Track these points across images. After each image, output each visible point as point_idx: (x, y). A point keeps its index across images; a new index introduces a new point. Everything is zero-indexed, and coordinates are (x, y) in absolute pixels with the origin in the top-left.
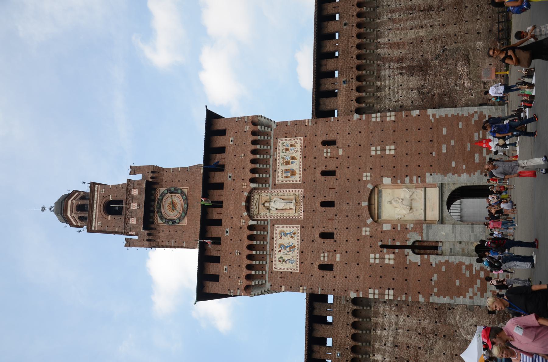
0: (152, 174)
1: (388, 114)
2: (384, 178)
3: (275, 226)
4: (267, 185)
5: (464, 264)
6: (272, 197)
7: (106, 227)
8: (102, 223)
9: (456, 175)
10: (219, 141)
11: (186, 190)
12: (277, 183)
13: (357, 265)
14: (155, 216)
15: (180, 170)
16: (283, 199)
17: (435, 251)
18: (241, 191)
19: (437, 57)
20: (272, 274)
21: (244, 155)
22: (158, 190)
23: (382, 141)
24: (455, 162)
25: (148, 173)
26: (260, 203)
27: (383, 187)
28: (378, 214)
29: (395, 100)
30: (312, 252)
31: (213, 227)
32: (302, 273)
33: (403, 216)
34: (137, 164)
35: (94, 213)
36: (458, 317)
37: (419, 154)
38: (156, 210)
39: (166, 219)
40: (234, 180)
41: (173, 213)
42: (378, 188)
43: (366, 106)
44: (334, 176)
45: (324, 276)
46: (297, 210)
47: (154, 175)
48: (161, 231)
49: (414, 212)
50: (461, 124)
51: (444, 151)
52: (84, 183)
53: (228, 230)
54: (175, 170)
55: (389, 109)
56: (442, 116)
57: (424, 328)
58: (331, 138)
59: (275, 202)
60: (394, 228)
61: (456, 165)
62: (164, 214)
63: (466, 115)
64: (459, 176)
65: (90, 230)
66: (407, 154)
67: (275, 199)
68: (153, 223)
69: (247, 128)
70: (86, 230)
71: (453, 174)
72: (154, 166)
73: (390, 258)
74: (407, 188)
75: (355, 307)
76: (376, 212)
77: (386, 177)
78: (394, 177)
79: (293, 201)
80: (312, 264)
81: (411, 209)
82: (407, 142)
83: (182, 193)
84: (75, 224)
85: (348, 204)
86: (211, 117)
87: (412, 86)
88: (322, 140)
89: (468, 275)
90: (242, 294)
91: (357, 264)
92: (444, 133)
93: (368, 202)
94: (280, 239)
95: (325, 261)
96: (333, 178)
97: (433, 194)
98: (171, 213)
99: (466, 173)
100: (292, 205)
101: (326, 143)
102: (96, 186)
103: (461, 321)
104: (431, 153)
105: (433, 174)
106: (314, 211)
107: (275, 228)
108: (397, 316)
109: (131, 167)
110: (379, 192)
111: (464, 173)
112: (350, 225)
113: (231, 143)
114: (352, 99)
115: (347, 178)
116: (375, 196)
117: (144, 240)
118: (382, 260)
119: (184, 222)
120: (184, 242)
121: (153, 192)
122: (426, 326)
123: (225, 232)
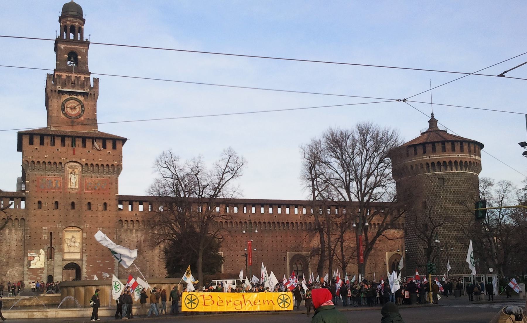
1: (118, 236)
5: (43, 271)
6: (77, 175)
7: (60, 53)
8: (62, 49)
9: (86, 267)
10: (109, 145)
11: (82, 118)
16: (76, 182)
19: (144, 258)
36: (17, 268)
38: (71, 97)
47: (92, 96)
48: (58, 100)
52: (90, 35)
53: (59, 150)
54: (95, 111)
57: (11, 253)
59: (75, 177)
62: (68, 102)
63: (115, 271)
64: (85, 268)
71: (86, 266)
79: (75, 187)
83: (80, 115)
86: (124, 141)
87: (131, 247)
89: (38, 272)
92: (106, 262)
97: (78, 256)
100: (73, 187)
101: (105, 204)
103: (16, 269)
104: (97, 256)
108: (16, 240)
110: (79, 231)
113: (108, 152)
119: (63, 116)
122: (12, 254)
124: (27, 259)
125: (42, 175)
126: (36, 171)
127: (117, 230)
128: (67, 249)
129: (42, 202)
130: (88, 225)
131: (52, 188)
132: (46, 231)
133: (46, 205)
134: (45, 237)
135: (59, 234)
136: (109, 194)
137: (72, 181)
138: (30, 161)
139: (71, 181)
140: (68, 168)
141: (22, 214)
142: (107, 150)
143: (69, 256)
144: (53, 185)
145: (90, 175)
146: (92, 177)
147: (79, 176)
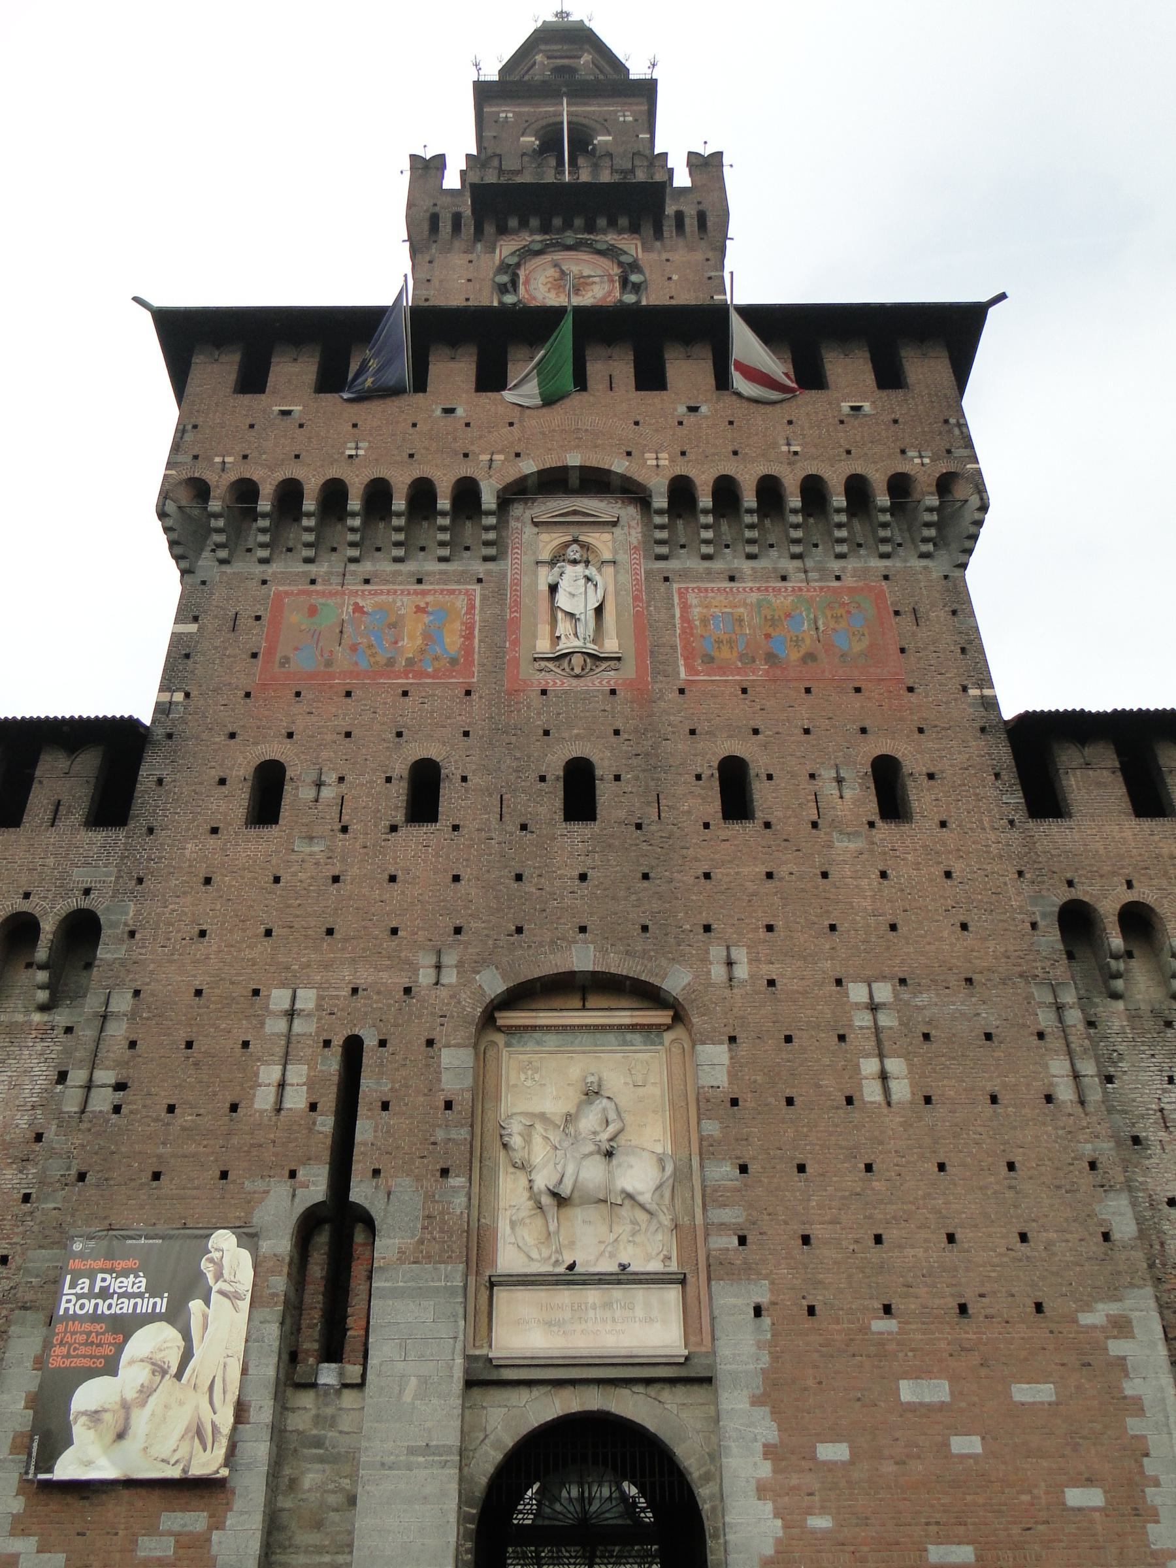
0: (694, 212)
2: (725, 1047)
3: (478, 587)
4: (664, 550)
5: (217, 1524)
6: (609, 570)
7: (495, 134)
12: (675, 586)
13: (262, 929)
14: (532, 234)
15: (715, 297)
16: (599, 611)
17: (316, 1346)
18: (629, 450)
20: (253, 584)
21: (796, 453)
22: (633, 239)
23: (926, 1037)
24: (843, 1463)
26: (584, 529)
27: (676, 1050)
28: (534, 1028)
29: (1167, 1107)
30: (348, 735)
31: (474, 366)
32: (248, 695)
33: (517, 1157)
37: (878, 1239)
39: (518, 265)
40: (680, 423)
41: (540, 285)
42: (669, 1028)
43: (1113, 957)
44: (720, 815)
45: (223, 789)
46: (550, 665)
47: (691, 223)
48: (470, 257)
49: (539, 1221)
50: (1091, 1504)
51: (908, 1392)
53: (460, 412)
55: (1109, 1079)
56: (1127, 1376)
58: (920, 797)
59: (588, 579)
60: (448, 1105)
61: (830, 1467)
66: (869, 1168)
67: (598, 578)
68: (503, 230)
69: (921, 457)
73: (288, 1088)
74: (681, 1177)
75: (48, 927)
76: (545, 1018)
77: (732, 1058)
78: (734, 1102)
79: (591, 648)
80: (290, 735)
81: (561, 1201)
82: (942, 1167)
85: (583, 877)
88: (898, 756)
90: (173, 472)
91: (268, 927)
92: (1022, 1393)
93: (594, 973)
94: (418, 607)
95: (297, 788)
96: (713, 807)
98: (542, 280)
99: (780, 1534)
104: (887, 1310)
105: (766, 1321)
106: (546, 733)
107: (469, 587)
111: (779, 1523)
112: (473, 892)
113: (845, 406)
114: (1135, 883)
115: (717, 874)
116: (628, 1013)
117: (435, 205)
118: (279, 1050)
121: (623, 221)
124: (40, 1362)
125: (313, 582)
126: (264, 553)
127: (1059, 1008)
128: (530, 1235)
129: (289, 773)
130: (740, 954)
131: (391, 662)
132: (299, 1026)
133: (327, 793)
134: (282, 1085)
135: (432, 1068)
136: (911, 690)
137: (562, 600)
138: (220, 483)
139: (554, 608)
140: (530, 530)
141: (81, 877)
142: (832, 394)
143: (549, 1323)
144: (405, 642)
145: (717, 565)
146: (732, 579)
147: (625, 578)
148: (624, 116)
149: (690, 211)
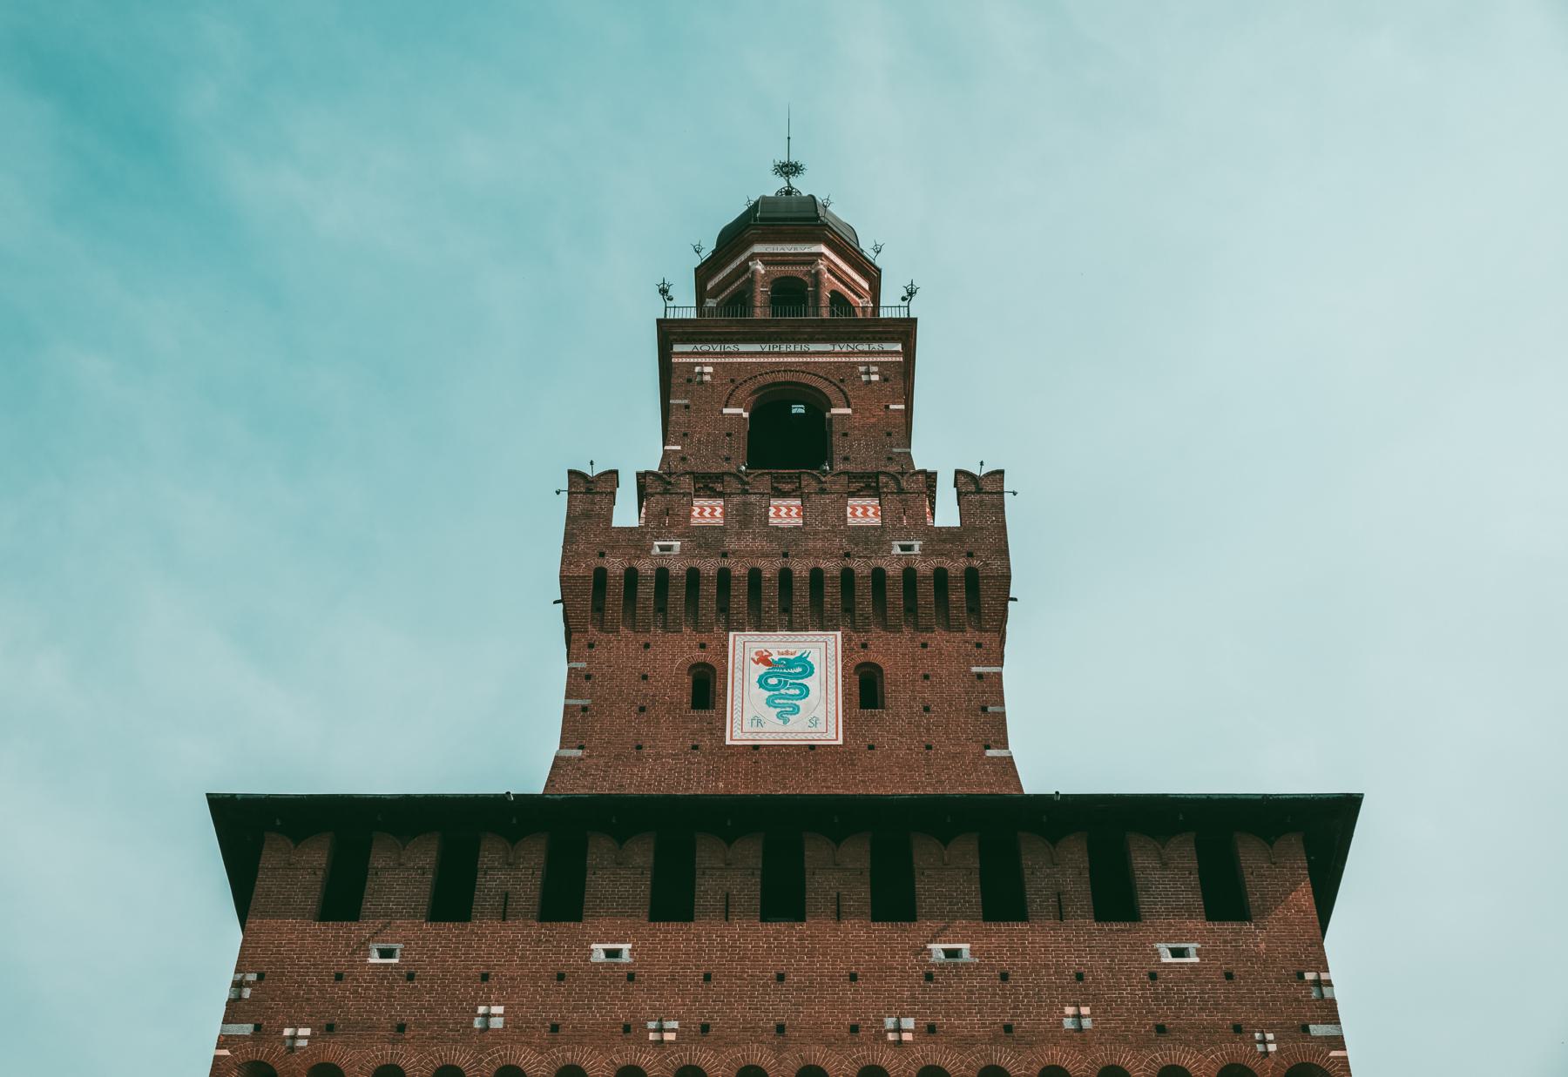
7: (686, 401)
8: (702, 382)
15: (990, 709)
25: (970, 555)
34: (1014, 512)
35: (756, 348)
53: (626, 958)
65: (669, 332)
70: (670, 316)
72: (1007, 578)
84: (709, 287)
90: (226, 1052)
102: (898, 347)
109: (999, 474)
120: (579, 753)
123: (613, 942)
148: (868, 373)
149: (956, 566)
